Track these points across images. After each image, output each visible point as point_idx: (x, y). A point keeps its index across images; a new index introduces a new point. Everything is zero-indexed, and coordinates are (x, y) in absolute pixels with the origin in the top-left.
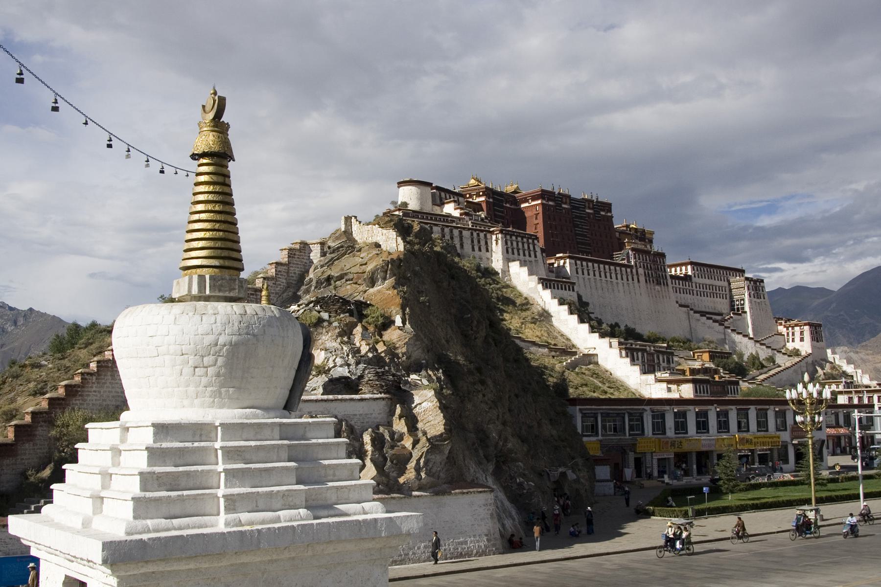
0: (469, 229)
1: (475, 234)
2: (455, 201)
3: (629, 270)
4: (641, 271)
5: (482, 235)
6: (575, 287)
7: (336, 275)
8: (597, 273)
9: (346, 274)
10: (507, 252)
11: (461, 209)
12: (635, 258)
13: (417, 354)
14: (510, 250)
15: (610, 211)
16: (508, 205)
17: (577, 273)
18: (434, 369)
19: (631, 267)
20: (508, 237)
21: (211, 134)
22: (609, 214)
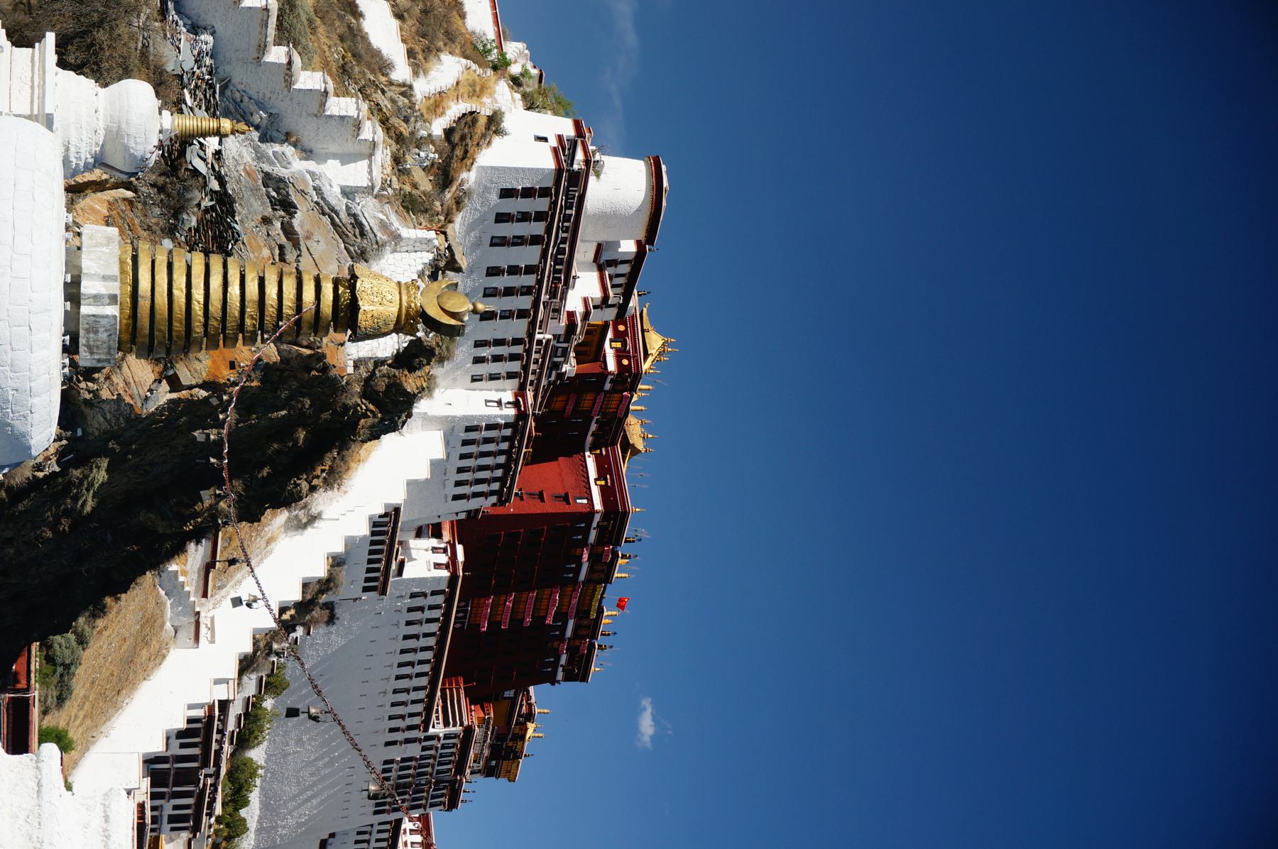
0: (531, 335)
1: (518, 349)
2: (605, 298)
3: (417, 721)
4: (414, 750)
5: (515, 366)
6: (374, 594)
7: (296, 222)
8: (412, 644)
9: (296, 245)
10: (468, 429)
11: (586, 315)
12: (446, 737)
13: (97, 422)
14: (472, 435)
15: (569, 677)
16: (593, 427)
17: (413, 596)
18: (61, 454)
19: (426, 730)
20: (508, 432)
21: (395, 310)
22: (560, 675)
